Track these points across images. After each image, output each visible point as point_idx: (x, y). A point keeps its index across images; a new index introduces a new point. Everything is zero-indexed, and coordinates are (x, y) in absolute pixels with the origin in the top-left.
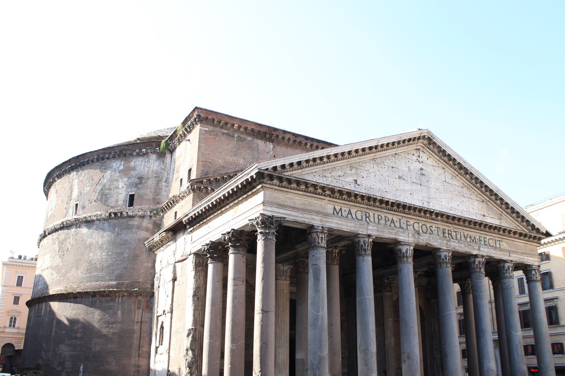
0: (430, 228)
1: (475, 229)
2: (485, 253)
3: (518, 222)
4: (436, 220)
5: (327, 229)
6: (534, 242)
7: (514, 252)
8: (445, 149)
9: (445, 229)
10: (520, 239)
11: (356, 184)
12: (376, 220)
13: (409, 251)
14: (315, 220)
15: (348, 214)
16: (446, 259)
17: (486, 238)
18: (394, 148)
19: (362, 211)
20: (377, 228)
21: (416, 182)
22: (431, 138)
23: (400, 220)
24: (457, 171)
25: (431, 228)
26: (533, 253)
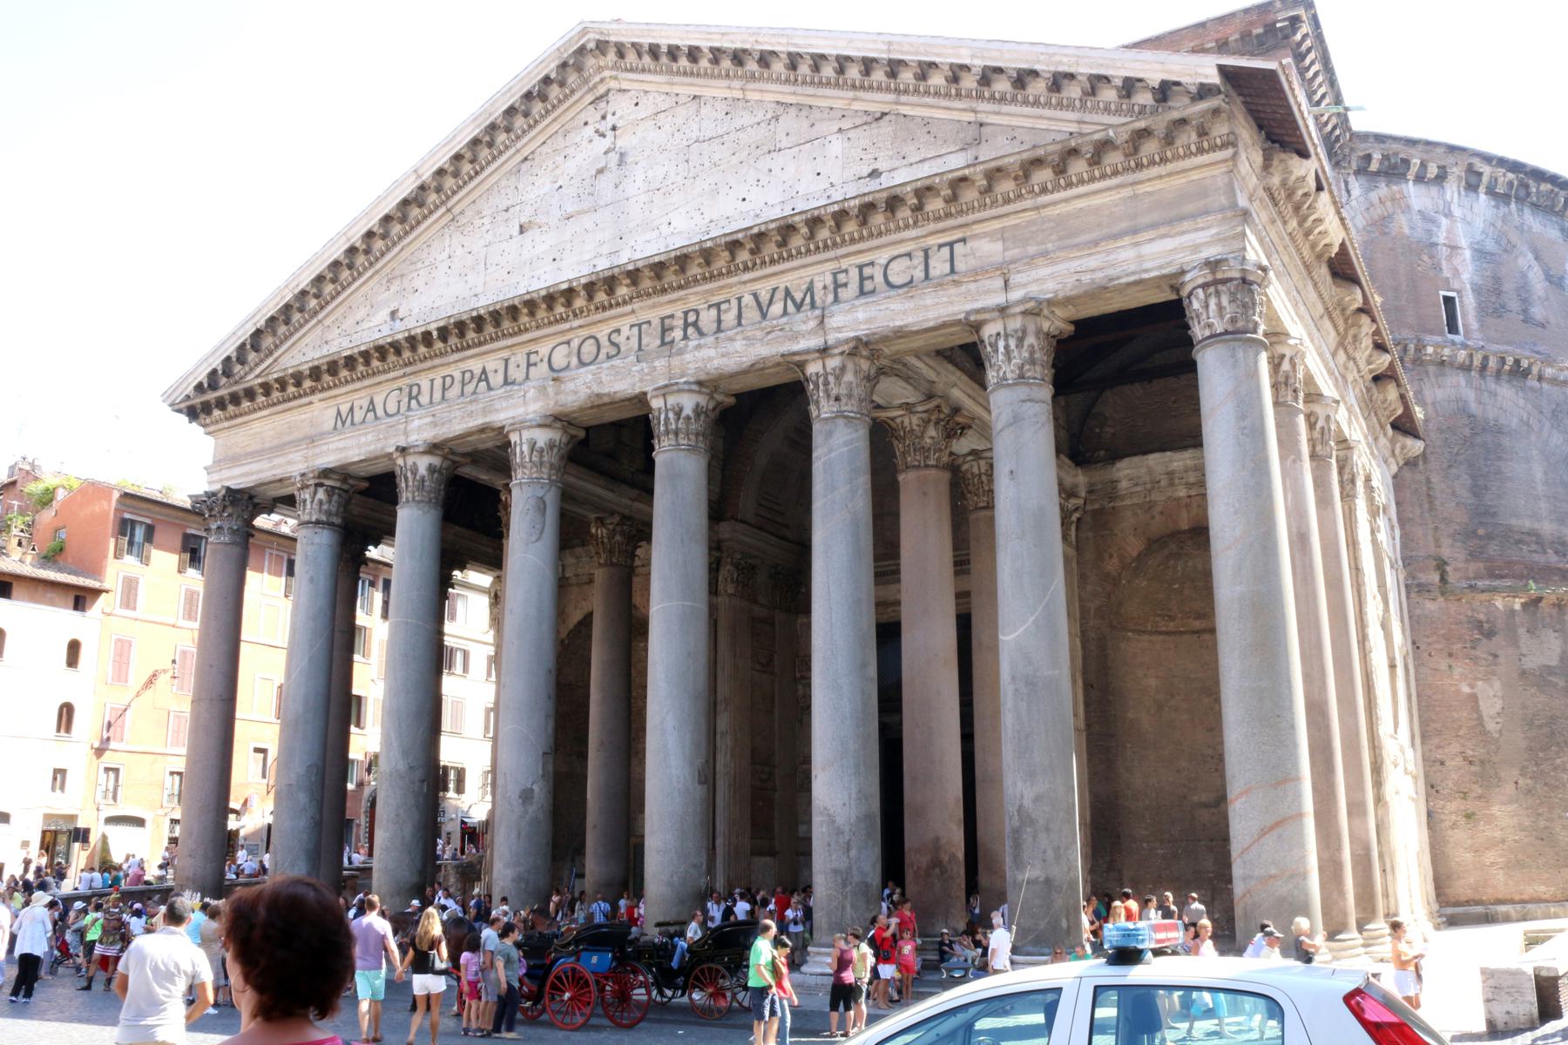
0: (609, 340)
1: (790, 256)
3: (1070, 106)
4: (618, 304)
6: (1177, 157)
7: (1033, 258)
8: (651, 41)
9: (672, 316)
10: (1070, 185)
12: (437, 395)
14: (294, 463)
15: (368, 411)
17: (872, 264)
18: (501, 153)
19: (400, 389)
22: (602, 38)
26: (1189, 208)
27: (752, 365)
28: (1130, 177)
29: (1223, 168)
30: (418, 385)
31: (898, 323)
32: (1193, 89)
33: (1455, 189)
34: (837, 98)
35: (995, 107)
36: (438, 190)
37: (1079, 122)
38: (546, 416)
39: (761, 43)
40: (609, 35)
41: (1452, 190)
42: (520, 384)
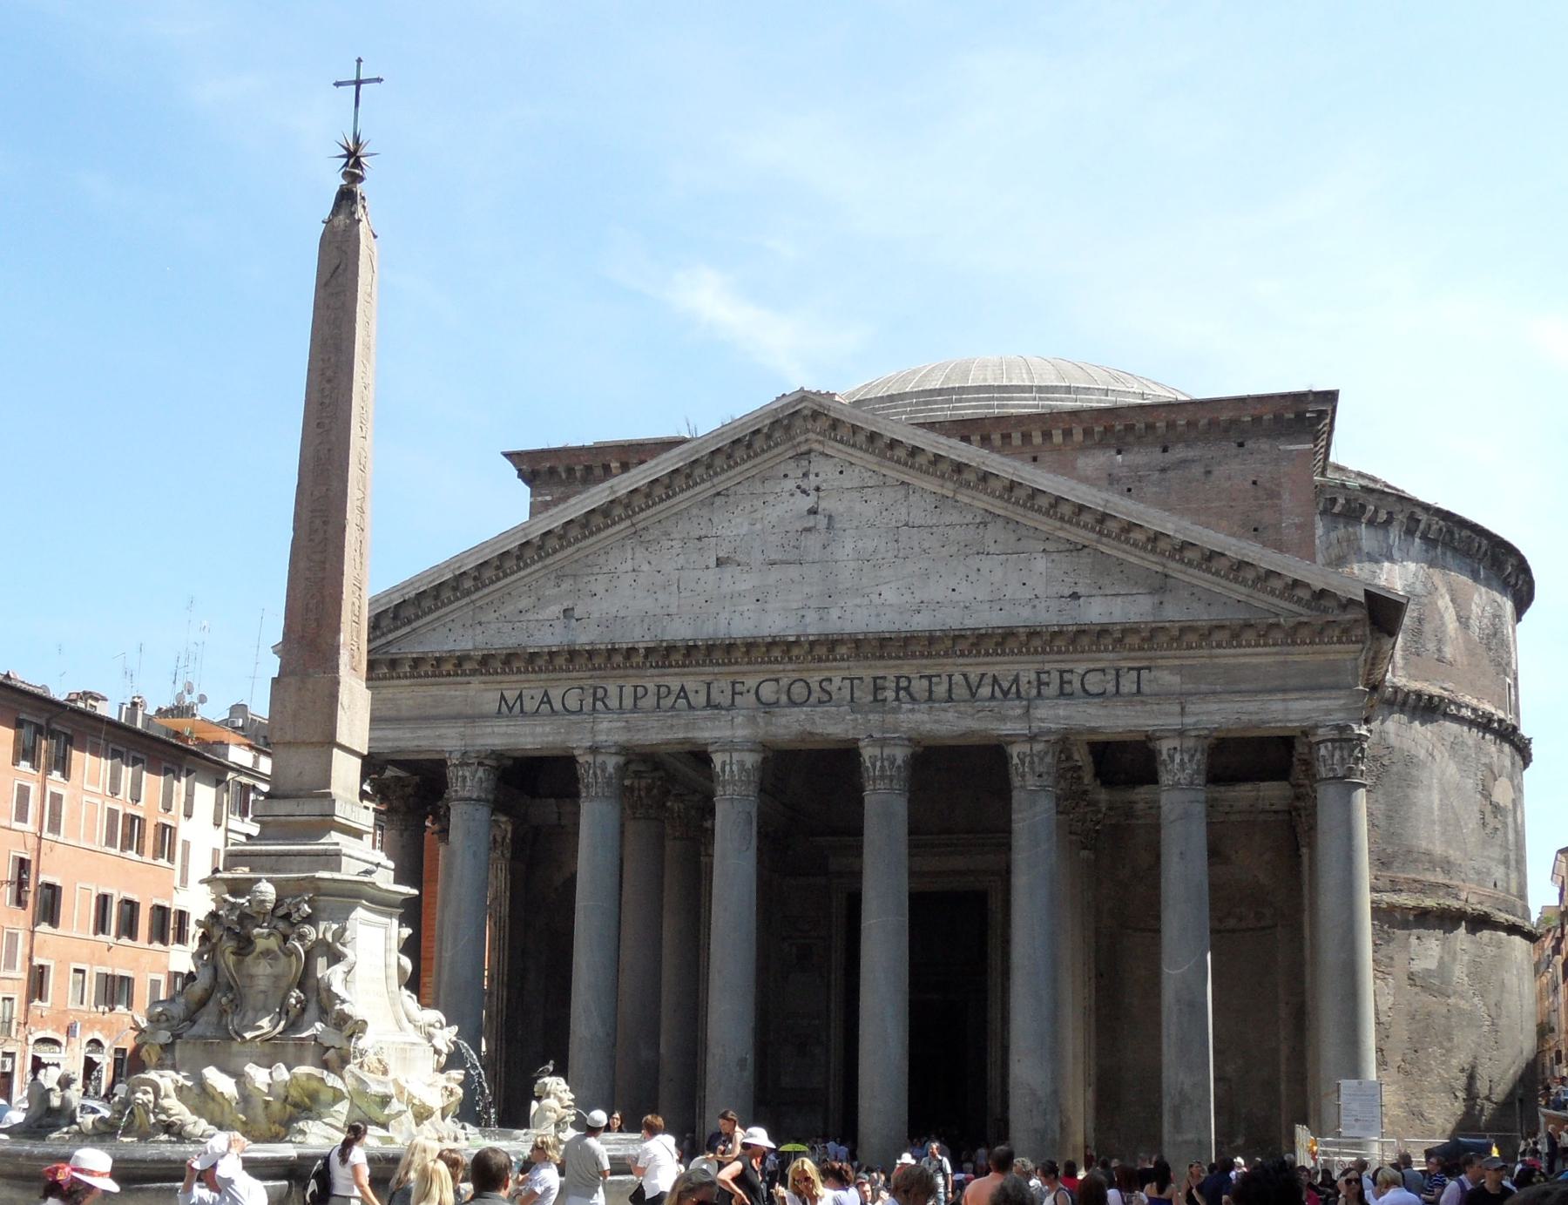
0: (821, 687)
1: (1004, 653)
2: (1059, 723)
3: (1244, 582)
4: (835, 660)
5: (473, 755)
6: (1321, 642)
7: (1206, 694)
8: (874, 429)
9: (884, 678)
10: (1239, 646)
11: (573, 617)
12: (628, 702)
13: (727, 768)
15: (542, 702)
16: (874, 770)
17: (1071, 671)
18: (696, 484)
20: (624, 724)
21: (784, 558)
23: (709, 685)
24: (950, 478)
25: (824, 684)
27: (961, 735)
28: (1285, 649)
29: (1352, 656)
30: (606, 691)
31: (1093, 724)
32: (1344, 601)
33: (1397, 533)
34: (1046, 524)
35: (1183, 567)
36: (627, 506)
37: (1248, 596)
38: (755, 742)
39: (987, 466)
40: (829, 410)
41: (1394, 534)
42: (728, 710)
